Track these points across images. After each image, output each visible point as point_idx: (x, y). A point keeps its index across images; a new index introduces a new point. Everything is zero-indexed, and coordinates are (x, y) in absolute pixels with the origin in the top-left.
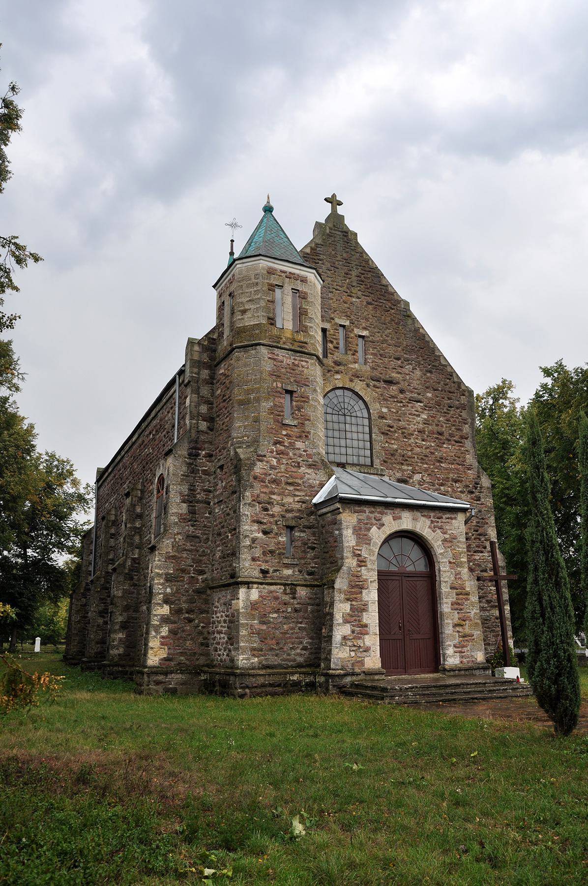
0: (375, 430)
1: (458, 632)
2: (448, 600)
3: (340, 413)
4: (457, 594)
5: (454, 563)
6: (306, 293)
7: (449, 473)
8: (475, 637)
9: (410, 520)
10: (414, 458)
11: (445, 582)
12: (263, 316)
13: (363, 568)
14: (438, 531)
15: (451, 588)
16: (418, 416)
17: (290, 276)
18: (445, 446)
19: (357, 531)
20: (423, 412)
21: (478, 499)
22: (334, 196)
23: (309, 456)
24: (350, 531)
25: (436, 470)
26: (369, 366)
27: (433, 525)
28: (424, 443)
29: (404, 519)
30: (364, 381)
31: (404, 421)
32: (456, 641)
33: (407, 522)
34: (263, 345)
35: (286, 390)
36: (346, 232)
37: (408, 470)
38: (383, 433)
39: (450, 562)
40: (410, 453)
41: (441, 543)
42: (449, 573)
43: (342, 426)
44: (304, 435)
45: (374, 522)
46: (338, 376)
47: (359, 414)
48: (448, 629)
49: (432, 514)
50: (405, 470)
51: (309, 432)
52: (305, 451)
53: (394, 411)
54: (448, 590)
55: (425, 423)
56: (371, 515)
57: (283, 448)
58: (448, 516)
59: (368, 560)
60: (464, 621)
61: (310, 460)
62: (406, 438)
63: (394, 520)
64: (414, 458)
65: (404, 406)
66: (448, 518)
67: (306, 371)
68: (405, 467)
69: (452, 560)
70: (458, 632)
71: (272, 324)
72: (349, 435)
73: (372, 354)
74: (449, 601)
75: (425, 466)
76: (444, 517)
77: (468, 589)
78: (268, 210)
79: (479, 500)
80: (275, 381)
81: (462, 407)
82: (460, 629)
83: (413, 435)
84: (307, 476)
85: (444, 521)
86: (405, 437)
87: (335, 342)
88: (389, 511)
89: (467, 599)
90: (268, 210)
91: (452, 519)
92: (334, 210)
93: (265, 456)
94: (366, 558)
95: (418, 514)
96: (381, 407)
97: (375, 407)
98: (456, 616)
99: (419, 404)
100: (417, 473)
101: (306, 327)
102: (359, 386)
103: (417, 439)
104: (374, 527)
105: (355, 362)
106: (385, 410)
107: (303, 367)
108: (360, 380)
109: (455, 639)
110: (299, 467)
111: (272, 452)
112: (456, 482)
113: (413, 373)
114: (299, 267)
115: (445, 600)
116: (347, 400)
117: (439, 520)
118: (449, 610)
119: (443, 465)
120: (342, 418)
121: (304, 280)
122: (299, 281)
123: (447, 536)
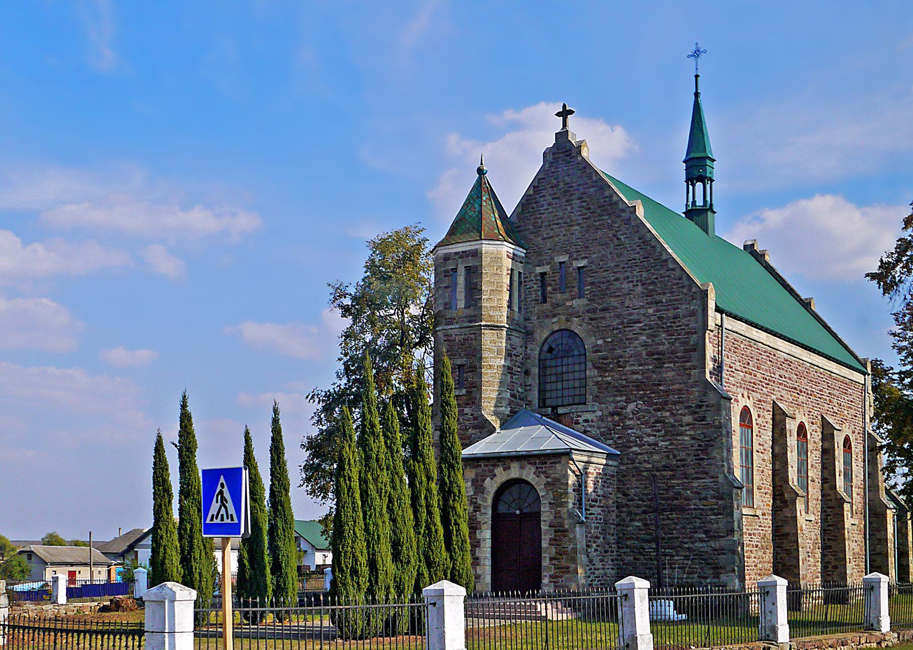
0: (589, 365)
1: (554, 564)
3: (558, 356)
4: (555, 532)
5: (554, 504)
6: (476, 267)
8: (571, 569)
9: (517, 469)
10: (629, 386)
11: (544, 521)
13: (478, 513)
14: (542, 476)
15: (550, 526)
16: (637, 339)
17: (464, 255)
18: (665, 365)
20: (641, 334)
21: (704, 418)
23: (475, 419)
25: (653, 395)
26: (587, 298)
27: (538, 471)
28: (641, 368)
31: (620, 349)
32: (552, 573)
33: (515, 472)
37: (621, 401)
38: (597, 368)
39: (550, 503)
40: (624, 382)
41: (543, 487)
42: (549, 513)
43: (559, 369)
46: (555, 320)
47: (576, 353)
48: (545, 563)
50: (618, 402)
51: (475, 398)
53: (610, 340)
56: (485, 468)
58: (552, 461)
59: (482, 506)
60: (561, 555)
61: (476, 422)
63: (504, 470)
66: (552, 463)
68: (619, 399)
70: (554, 564)
72: (565, 377)
75: (642, 392)
76: (548, 463)
77: (567, 527)
79: (703, 420)
82: (555, 562)
83: (629, 361)
84: (473, 436)
86: (620, 366)
87: (553, 283)
88: (500, 464)
90: (480, 171)
91: (555, 463)
94: (480, 504)
95: (526, 463)
96: (597, 340)
99: (637, 325)
100: (632, 402)
102: (575, 325)
103: (633, 365)
105: (572, 300)
108: (576, 317)
109: (551, 571)
112: (675, 404)
113: (634, 291)
115: (543, 537)
118: (547, 545)
119: (661, 388)
120: (559, 361)
123: (549, 480)
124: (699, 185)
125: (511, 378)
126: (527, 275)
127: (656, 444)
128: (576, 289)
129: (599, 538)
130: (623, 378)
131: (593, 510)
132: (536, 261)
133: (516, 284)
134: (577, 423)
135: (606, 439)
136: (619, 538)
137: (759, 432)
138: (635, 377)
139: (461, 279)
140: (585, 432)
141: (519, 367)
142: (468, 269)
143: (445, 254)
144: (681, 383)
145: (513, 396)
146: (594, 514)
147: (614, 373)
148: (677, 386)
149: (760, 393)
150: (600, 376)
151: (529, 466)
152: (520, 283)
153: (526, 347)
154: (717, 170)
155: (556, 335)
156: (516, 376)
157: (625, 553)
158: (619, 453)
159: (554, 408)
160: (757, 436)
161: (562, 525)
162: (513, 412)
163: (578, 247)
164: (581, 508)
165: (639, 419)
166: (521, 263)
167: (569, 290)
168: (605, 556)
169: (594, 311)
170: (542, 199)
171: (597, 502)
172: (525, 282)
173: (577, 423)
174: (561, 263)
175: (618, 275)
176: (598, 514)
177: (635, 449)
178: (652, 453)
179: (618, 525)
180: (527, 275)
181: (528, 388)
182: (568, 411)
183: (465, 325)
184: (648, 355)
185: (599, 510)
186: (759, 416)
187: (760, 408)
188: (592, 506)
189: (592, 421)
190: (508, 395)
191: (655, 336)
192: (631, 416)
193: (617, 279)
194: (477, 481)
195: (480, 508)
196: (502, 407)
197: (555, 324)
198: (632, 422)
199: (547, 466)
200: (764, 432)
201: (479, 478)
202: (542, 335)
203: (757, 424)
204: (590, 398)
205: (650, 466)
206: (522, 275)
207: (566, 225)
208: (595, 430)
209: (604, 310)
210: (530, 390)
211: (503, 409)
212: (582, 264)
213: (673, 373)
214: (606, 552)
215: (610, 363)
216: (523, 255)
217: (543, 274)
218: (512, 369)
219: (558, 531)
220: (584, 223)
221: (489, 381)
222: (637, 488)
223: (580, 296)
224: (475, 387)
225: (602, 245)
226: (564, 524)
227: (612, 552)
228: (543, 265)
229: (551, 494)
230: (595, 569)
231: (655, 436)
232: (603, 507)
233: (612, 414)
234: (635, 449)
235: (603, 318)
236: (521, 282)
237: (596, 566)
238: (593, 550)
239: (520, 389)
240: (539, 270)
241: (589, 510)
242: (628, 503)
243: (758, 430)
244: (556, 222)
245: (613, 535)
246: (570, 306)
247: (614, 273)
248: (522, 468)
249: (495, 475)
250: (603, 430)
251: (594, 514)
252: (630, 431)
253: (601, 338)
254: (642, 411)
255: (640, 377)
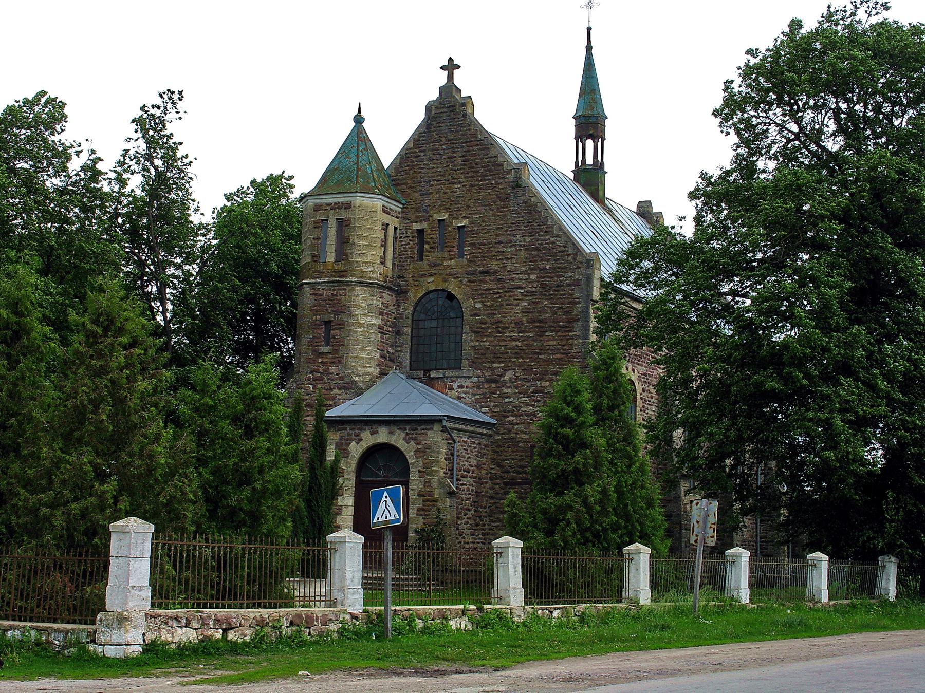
0: (466, 329)
2: (414, 507)
6: (349, 220)
7: (549, 365)
12: (309, 255)
15: (418, 495)
16: (517, 305)
17: (336, 207)
18: (547, 334)
19: (338, 445)
20: (522, 300)
22: (450, 59)
23: (341, 378)
24: (333, 447)
29: (380, 434)
30: (458, 278)
33: (383, 436)
34: (306, 283)
35: (324, 321)
36: (453, 106)
38: (474, 332)
39: (419, 471)
44: (338, 361)
45: (354, 437)
46: (432, 279)
49: (408, 427)
51: (342, 357)
52: (337, 374)
54: (416, 496)
55: (524, 312)
56: (351, 432)
57: (319, 375)
62: (500, 333)
64: (508, 353)
65: (500, 297)
66: (423, 429)
67: (343, 298)
68: (496, 365)
69: (422, 469)
71: (315, 261)
73: (471, 245)
74: (415, 507)
76: (419, 428)
78: (359, 119)
80: (315, 315)
81: (577, 283)
83: (509, 328)
85: (419, 432)
87: (431, 241)
88: (367, 427)
89: (434, 506)
90: (359, 119)
91: (426, 429)
92: (450, 77)
93: (303, 384)
97: (468, 305)
98: (421, 520)
101: (347, 255)
103: (513, 331)
104: (354, 442)
105: (451, 259)
106: (478, 305)
107: (341, 295)
110: (332, 390)
111: (309, 379)
114: (342, 195)
116: (441, 302)
117: (414, 432)
118: (415, 515)
119: (542, 357)
121: (348, 206)
122: (343, 210)
124: (589, 143)
125: (382, 338)
126: (404, 231)
127: (535, 415)
128: (455, 249)
129: (470, 510)
130: (502, 343)
131: (464, 481)
132: (413, 217)
133: (391, 240)
134: (451, 389)
135: (481, 407)
136: (491, 511)
137: (644, 407)
138: (514, 344)
139: (332, 231)
140: (459, 398)
141: (390, 326)
142: (340, 222)
143: (316, 205)
144: (563, 354)
145: (381, 356)
146: (465, 485)
147: (492, 339)
148: (558, 356)
149: (645, 367)
150: (477, 341)
151: (398, 431)
152: (395, 238)
153: (399, 306)
154: (611, 129)
155: (431, 296)
156: (387, 336)
157: (497, 527)
158: (496, 422)
159: (427, 371)
160: (641, 411)
161: (431, 494)
162: (383, 374)
163: (460, 206)
164: (452, 478)
165: (517, 387)
166: (397, 217)
167: (448, 249)
168: (475, 530)
169: (473, 273)
170: (423, 154)
171: (469, 472)
172: (401, 238)
173: (451, 389)
174: (439, 221)
175: (500, 238)
176: (470, 485)
177: (511, 418)
178: (529, 423)
179: (491, 498)
180: (404, 231)
181: (399, 349)
182: (441, 376)
183: (334, 279)
184: (528, 322)
185: (471, 481)
186: (644, 390)
187: (645, 382)
188: (463, 477)
189: (467, 387)
190: (378, 355)
191: (538, 303)
192: (508, 385)
193: (500, 242)
194: (341, 444)
195: (343, 473)
196: (370, 367)
197: (431, 283)
198: (509, 391)
199: (419, 432)
200: (649, 407)
201: (344, 442)
202: (414, 295)
203: (641, 398)
204: (465, 363)
205: (527, 437)
206: (398, 230)
207: (447, 183)
208: (470, 396)
209: (487, 272)
210: (401, 351)
211: (372, 369)
212: (465, 222)
213: (555, 343)
214: (477, 525)
215: (488, 328)
216: (400, 210)
217: (420, 232)
218: (382, 329)
219: (428, 501)
220: (468, 181)
221: (358, 340)
222: (513, 459)
223: (461, 255)
224: (343, 345)
225: (485, 206)
226: (434, 494)
227: (484, 525)
228: (421, 221)
229: (421, 462)
230: (464, 543)
231: (533, 406)
232: (475, 478)
233: (489, 381)
234: (511, 418)
235: (484, 282)
236: (396, 238)
237: (467, 540)
238: (463, 522)
239: (390, 350)
240: (416, 226)
241: (460, 480)
242: (503, 475)
243: (642, 404)
244: (436, 178)
245: (485, 508)
246: (448, 266)
247: (497, 235)
248: (391, 433)
249: (362, 440)
250: (478, 397)
251: (465, 485)
252: (507, 400)
253: (479, 302)
254: (521, 379)
255: (520, 344)
